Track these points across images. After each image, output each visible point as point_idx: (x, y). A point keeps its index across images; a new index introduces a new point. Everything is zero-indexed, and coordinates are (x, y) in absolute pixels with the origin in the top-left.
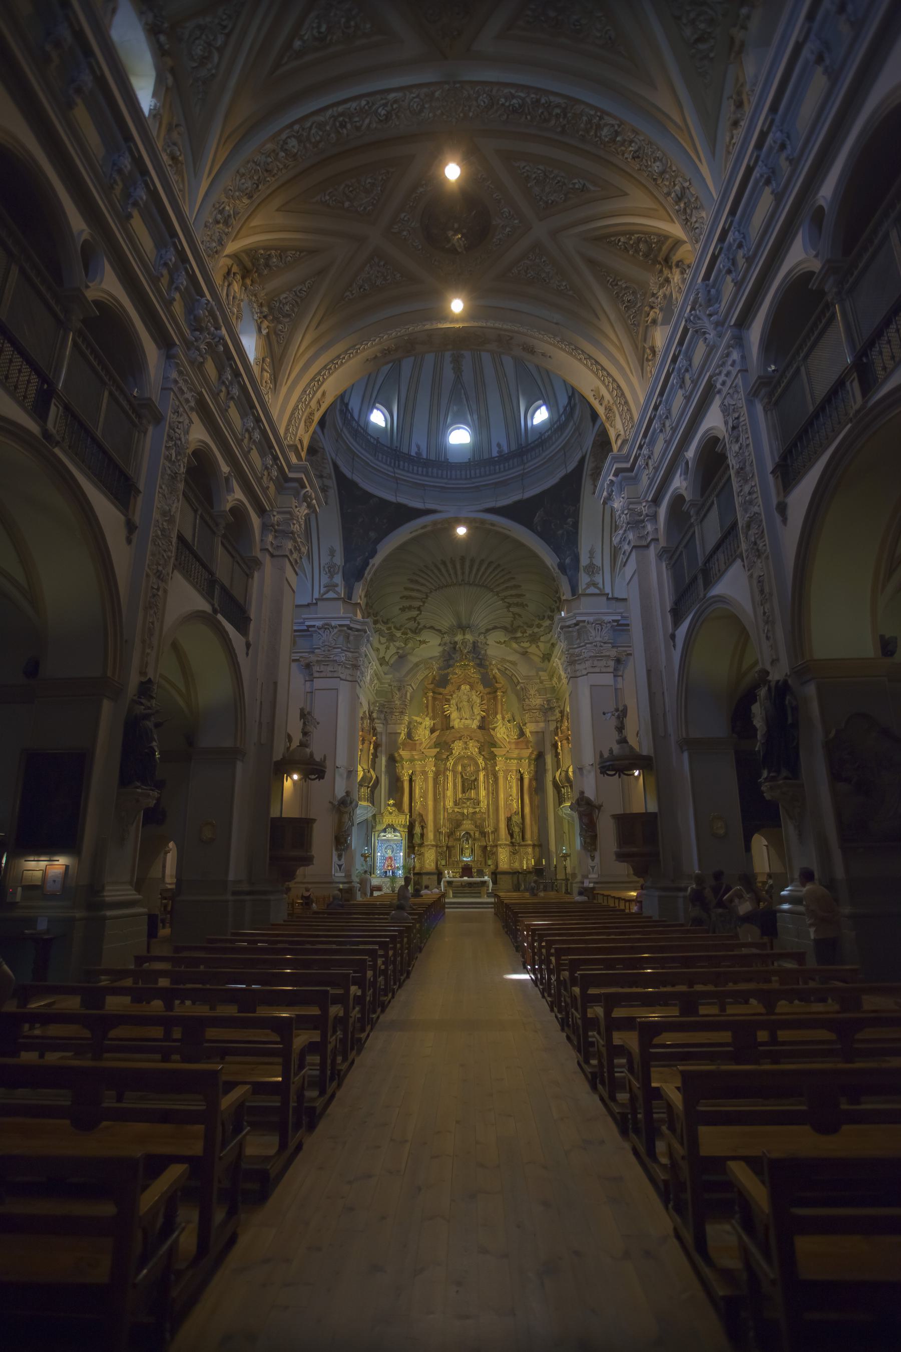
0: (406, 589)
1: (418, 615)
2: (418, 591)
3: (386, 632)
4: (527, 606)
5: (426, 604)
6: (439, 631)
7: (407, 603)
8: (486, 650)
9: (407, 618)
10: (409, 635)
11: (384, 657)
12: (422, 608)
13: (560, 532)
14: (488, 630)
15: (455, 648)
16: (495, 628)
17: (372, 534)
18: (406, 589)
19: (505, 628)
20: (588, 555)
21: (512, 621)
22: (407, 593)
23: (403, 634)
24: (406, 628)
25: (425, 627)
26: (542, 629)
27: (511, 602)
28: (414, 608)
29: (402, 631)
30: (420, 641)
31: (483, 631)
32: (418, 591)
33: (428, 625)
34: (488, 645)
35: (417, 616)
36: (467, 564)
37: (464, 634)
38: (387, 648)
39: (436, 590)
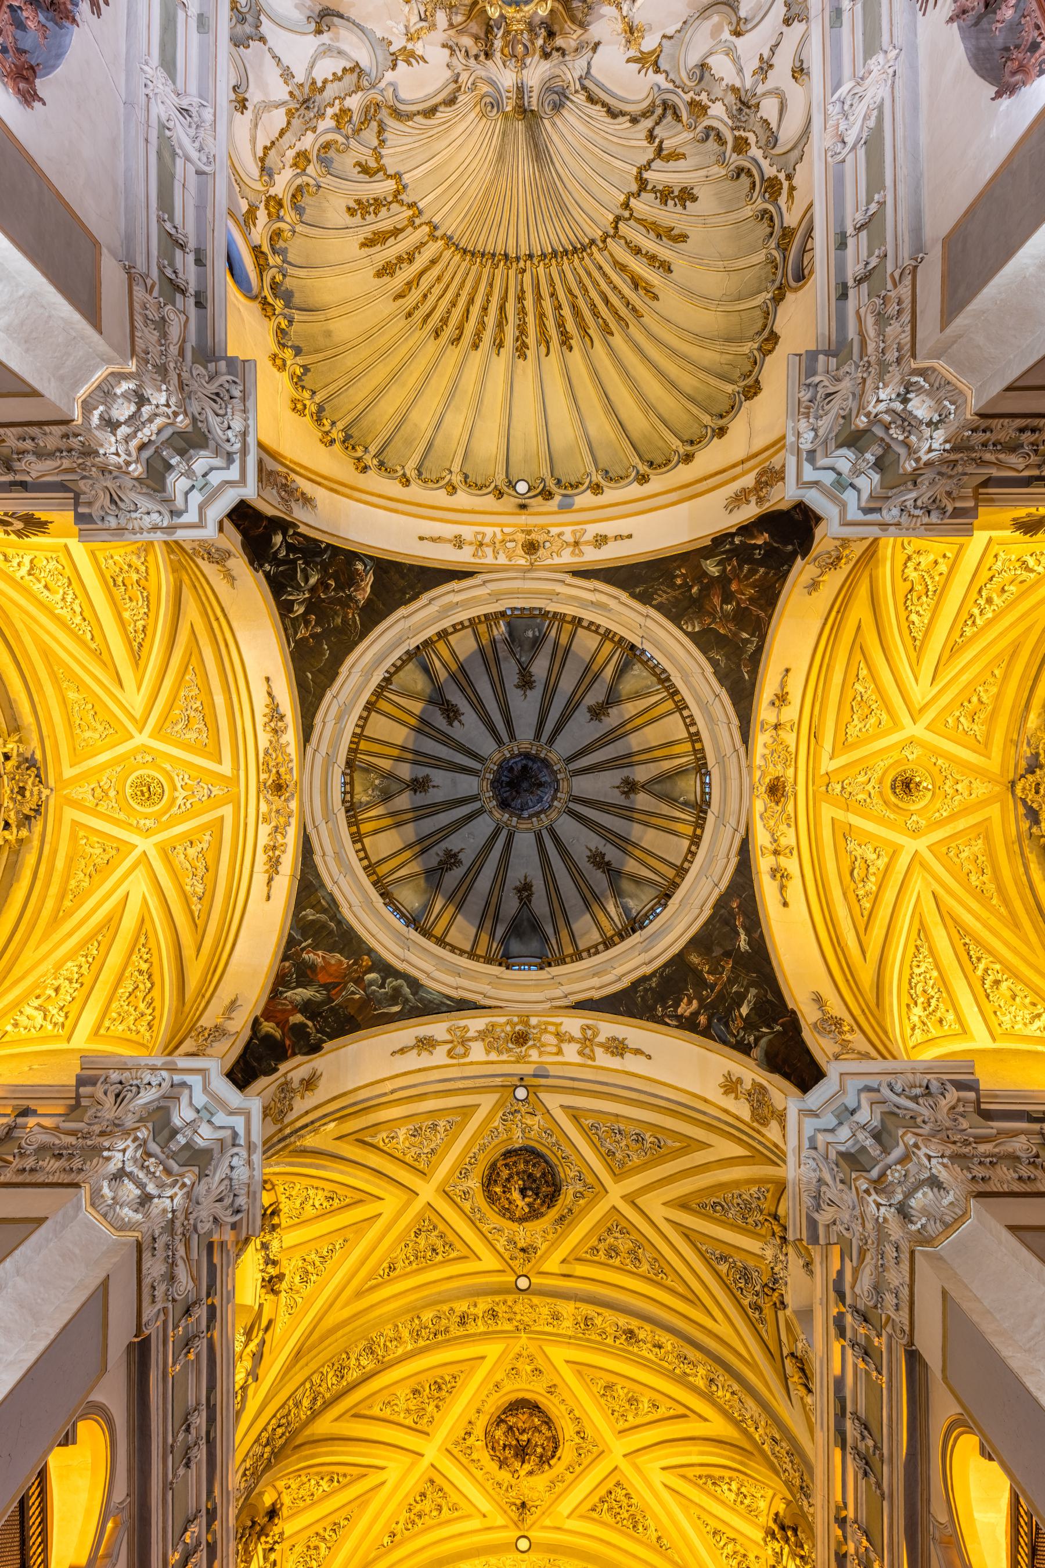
0: (666, 267)
1: (648, 166)
2: (637, 251)
3: (752, 138)
4: (349, 209)
5: (622, 198)
6: (591, 99)
7: (669, 216)
8: (451, 26)
9: (681, 164)
10: (687, 97)
11: (787, 22)
12: (634, 187)
13: (313, 581)
14: (451, 101)
15: (551, 35)
16: (430, 112)
17: (712, 568)
18: (666, 267)
19: (398, 114)
20: (233, 573)
21: (382, 142)
22: (663, 251)
23: (704, 109)
24: (689, 127)
25: (634, 121)
26: (291, 154)
27: (395, 206)
28: (654, 190)
29: (706, 123)
30: (657, 71)
31: (462, 98)
32: (637, 251)
33: (624, 123)
34: (444, 46)
35: (649, 163)
36: (510, 331)
37: (520, 89)
38: (765, 67)
39: (593, 242)
